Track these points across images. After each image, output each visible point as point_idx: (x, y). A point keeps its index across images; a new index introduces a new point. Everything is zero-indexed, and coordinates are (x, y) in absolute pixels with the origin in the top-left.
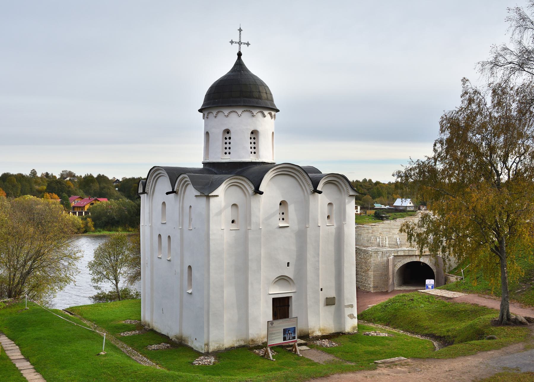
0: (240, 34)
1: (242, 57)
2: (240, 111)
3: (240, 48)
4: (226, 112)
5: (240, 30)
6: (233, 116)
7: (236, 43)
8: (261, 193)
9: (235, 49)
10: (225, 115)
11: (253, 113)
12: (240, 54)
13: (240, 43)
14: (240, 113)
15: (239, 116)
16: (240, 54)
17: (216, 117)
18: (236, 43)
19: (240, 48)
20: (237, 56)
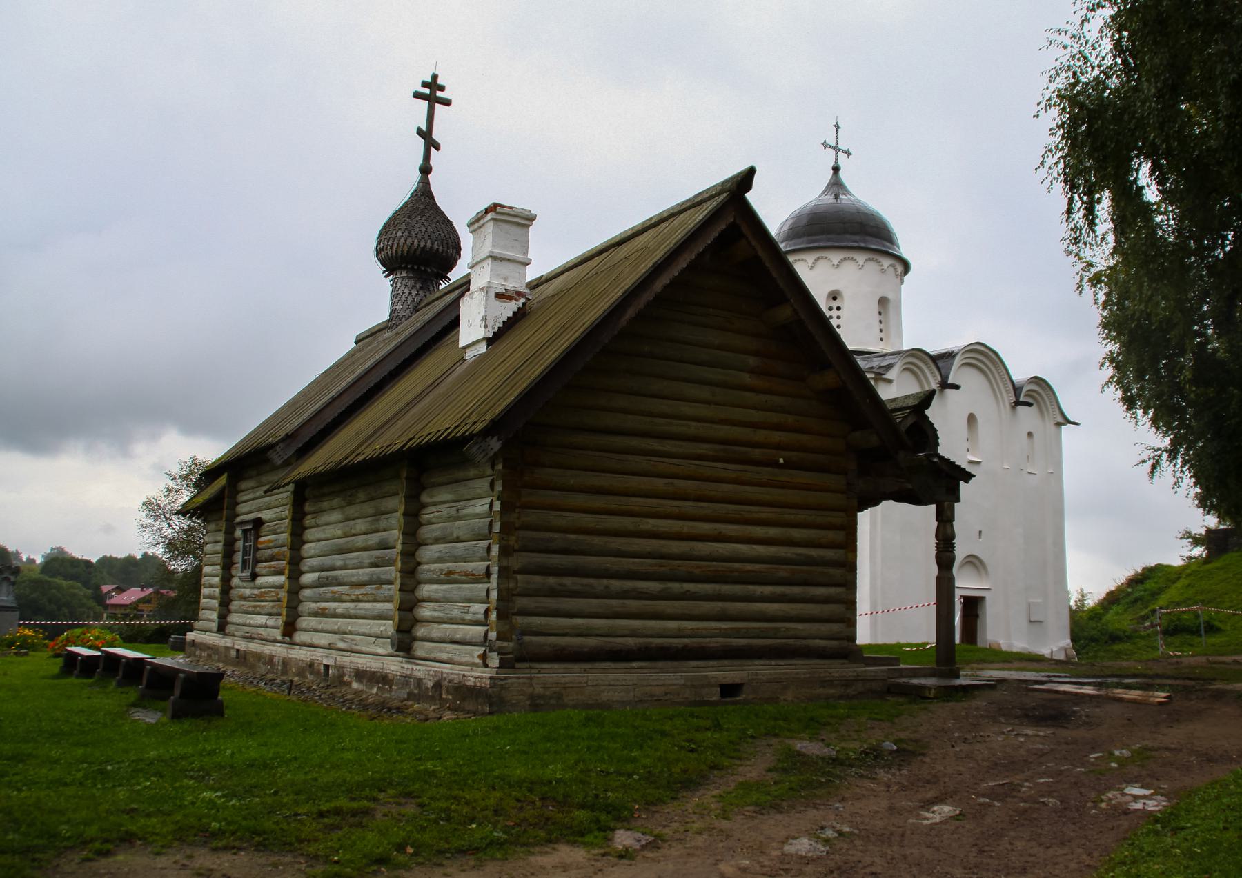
0: (837, 133)
1: (841, 173)
2: (861, 258)
3: (836, 157)
4: (836, 257)
5: (837, 127)
6: (849, 267)
8: (957, 387)
9: (829, 158)
10: (834, 265)
12: (836, 169)
13: (836, 149)
16: (836, 169)
17: (812, 268)
19: (836, 157)
20: (832, 172)
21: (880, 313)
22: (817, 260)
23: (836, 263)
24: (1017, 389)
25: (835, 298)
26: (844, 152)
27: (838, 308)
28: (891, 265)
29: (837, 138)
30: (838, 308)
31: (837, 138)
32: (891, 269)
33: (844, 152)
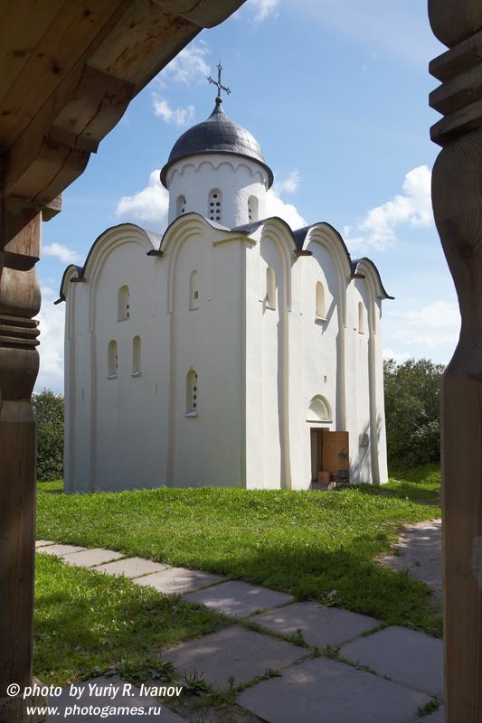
7: (215, 83)
11: (251, 172)
12: (218, 101)
14: (235, 167)
15: (234, 171)
16: (218, 101)
18: (215, 83)
20: (215, 104)
21: (250, 210)
22: (204, 163)
23: (216, 166)
24: (353, 265)
25: (215, 196)
26: (225, 89)
27: (218, 204)
28: (258, 172)
29: (219, 76)
30: (218, 204)
31: (219, 76)
32: (258, 175)
33: (225, 89)
